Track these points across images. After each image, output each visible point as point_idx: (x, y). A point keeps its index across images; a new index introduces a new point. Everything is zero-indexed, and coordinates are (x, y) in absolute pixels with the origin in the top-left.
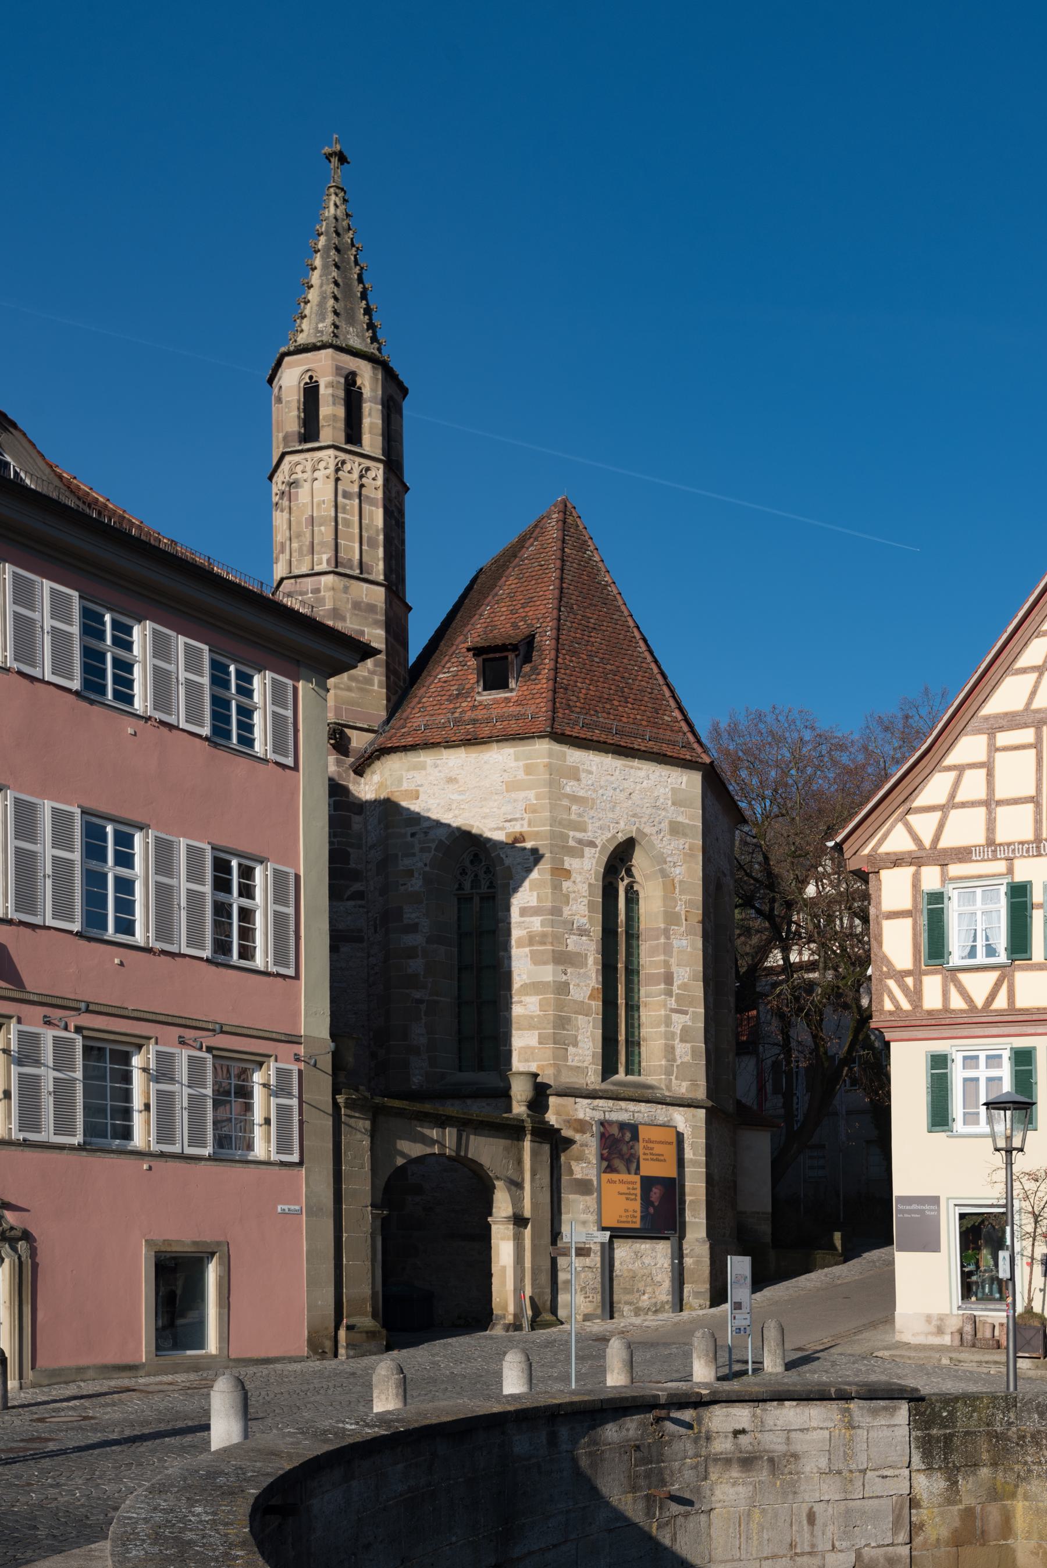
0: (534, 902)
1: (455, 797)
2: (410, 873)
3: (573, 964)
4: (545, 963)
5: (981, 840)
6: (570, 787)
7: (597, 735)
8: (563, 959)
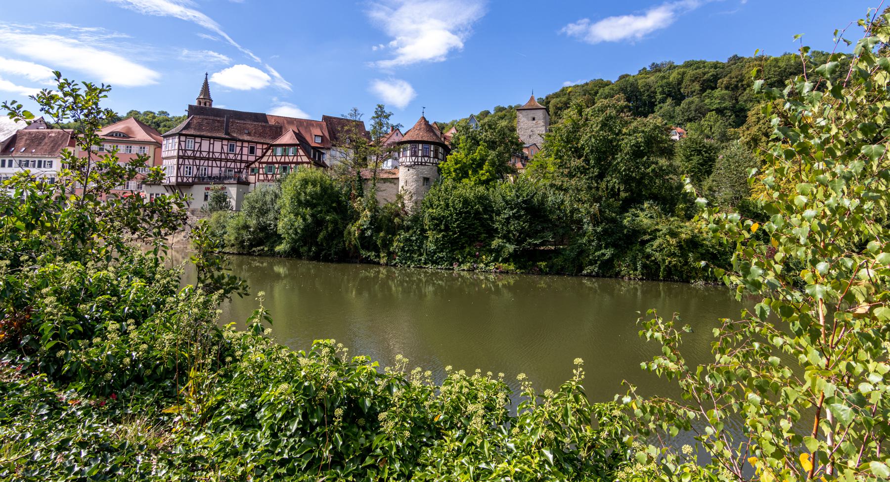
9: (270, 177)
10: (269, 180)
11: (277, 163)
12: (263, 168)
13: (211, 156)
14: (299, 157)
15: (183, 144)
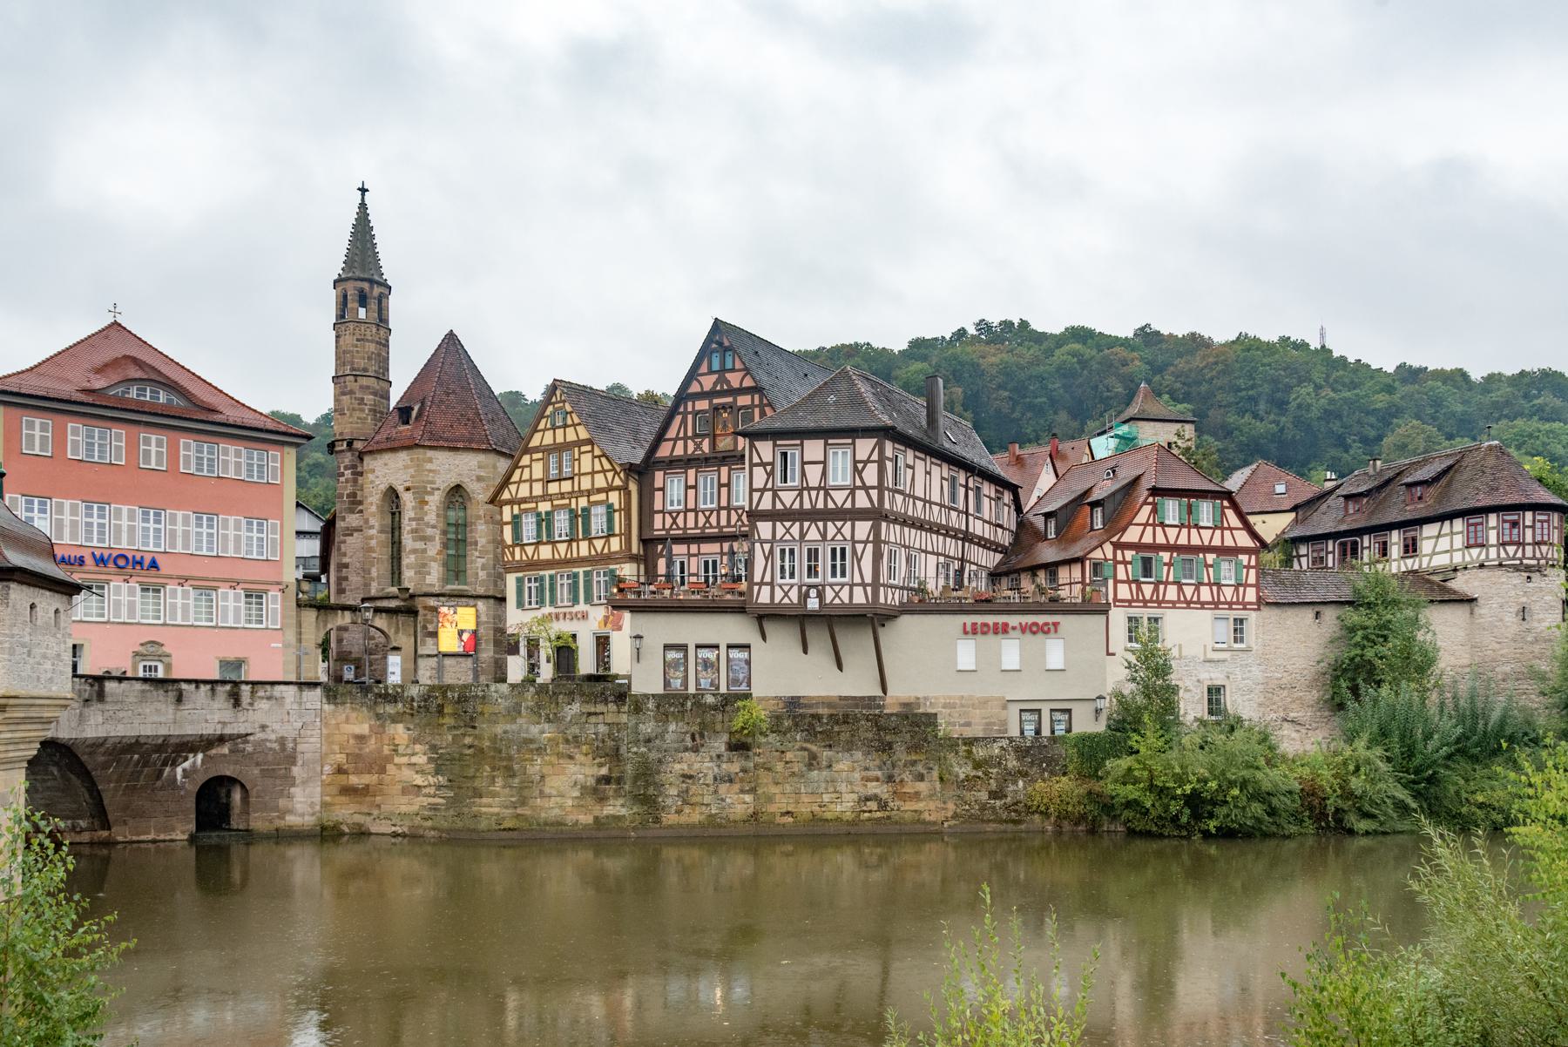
0: (413, 516)
2: (371, 504)
3: (429, 541)
5: (528, 495)
6: (429, 466)
7: (441, 443)
9: (1148, 590)
10: (1145, 602)
11: (1167, 547)
12: (1125, 563)
13: (927, 518)
14: (1227, 533)
15: (889, 465)
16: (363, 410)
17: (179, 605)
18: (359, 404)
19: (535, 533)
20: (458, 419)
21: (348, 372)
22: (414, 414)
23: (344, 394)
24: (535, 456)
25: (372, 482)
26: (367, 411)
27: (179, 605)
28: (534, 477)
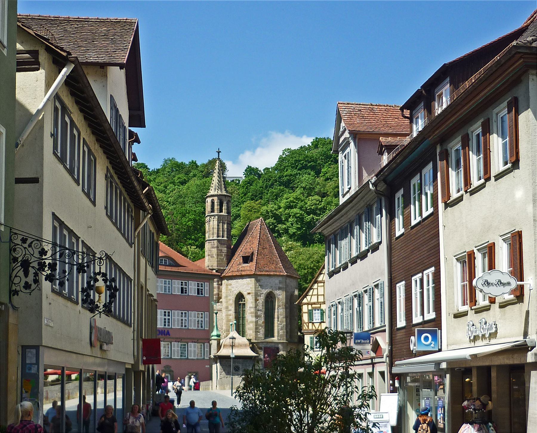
0: (251, 306)
1: (238, 285)
3: (259, 317)
4: (253, 317)
5: (316, 301)
7: (264, 273)
8: (257, 316)
16: (222, 255)
17: (176, 350)
18: (220, 252)
19: (320, 318)
20: (270, 261)
21: (215, 238)
22: (250, 258)
23: (213, 248)
24: (319, 284)
25: (230, 290)
26: (223, 255)
27: (176, 350)
28: (319, 294)
